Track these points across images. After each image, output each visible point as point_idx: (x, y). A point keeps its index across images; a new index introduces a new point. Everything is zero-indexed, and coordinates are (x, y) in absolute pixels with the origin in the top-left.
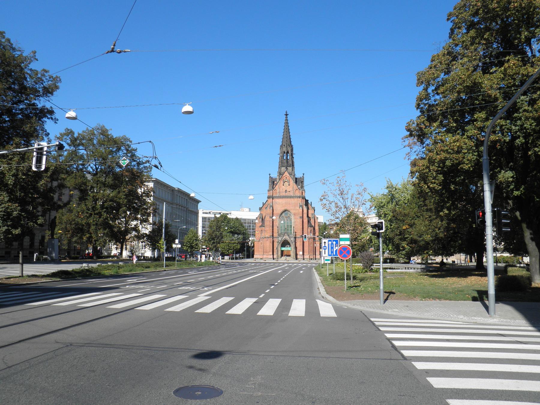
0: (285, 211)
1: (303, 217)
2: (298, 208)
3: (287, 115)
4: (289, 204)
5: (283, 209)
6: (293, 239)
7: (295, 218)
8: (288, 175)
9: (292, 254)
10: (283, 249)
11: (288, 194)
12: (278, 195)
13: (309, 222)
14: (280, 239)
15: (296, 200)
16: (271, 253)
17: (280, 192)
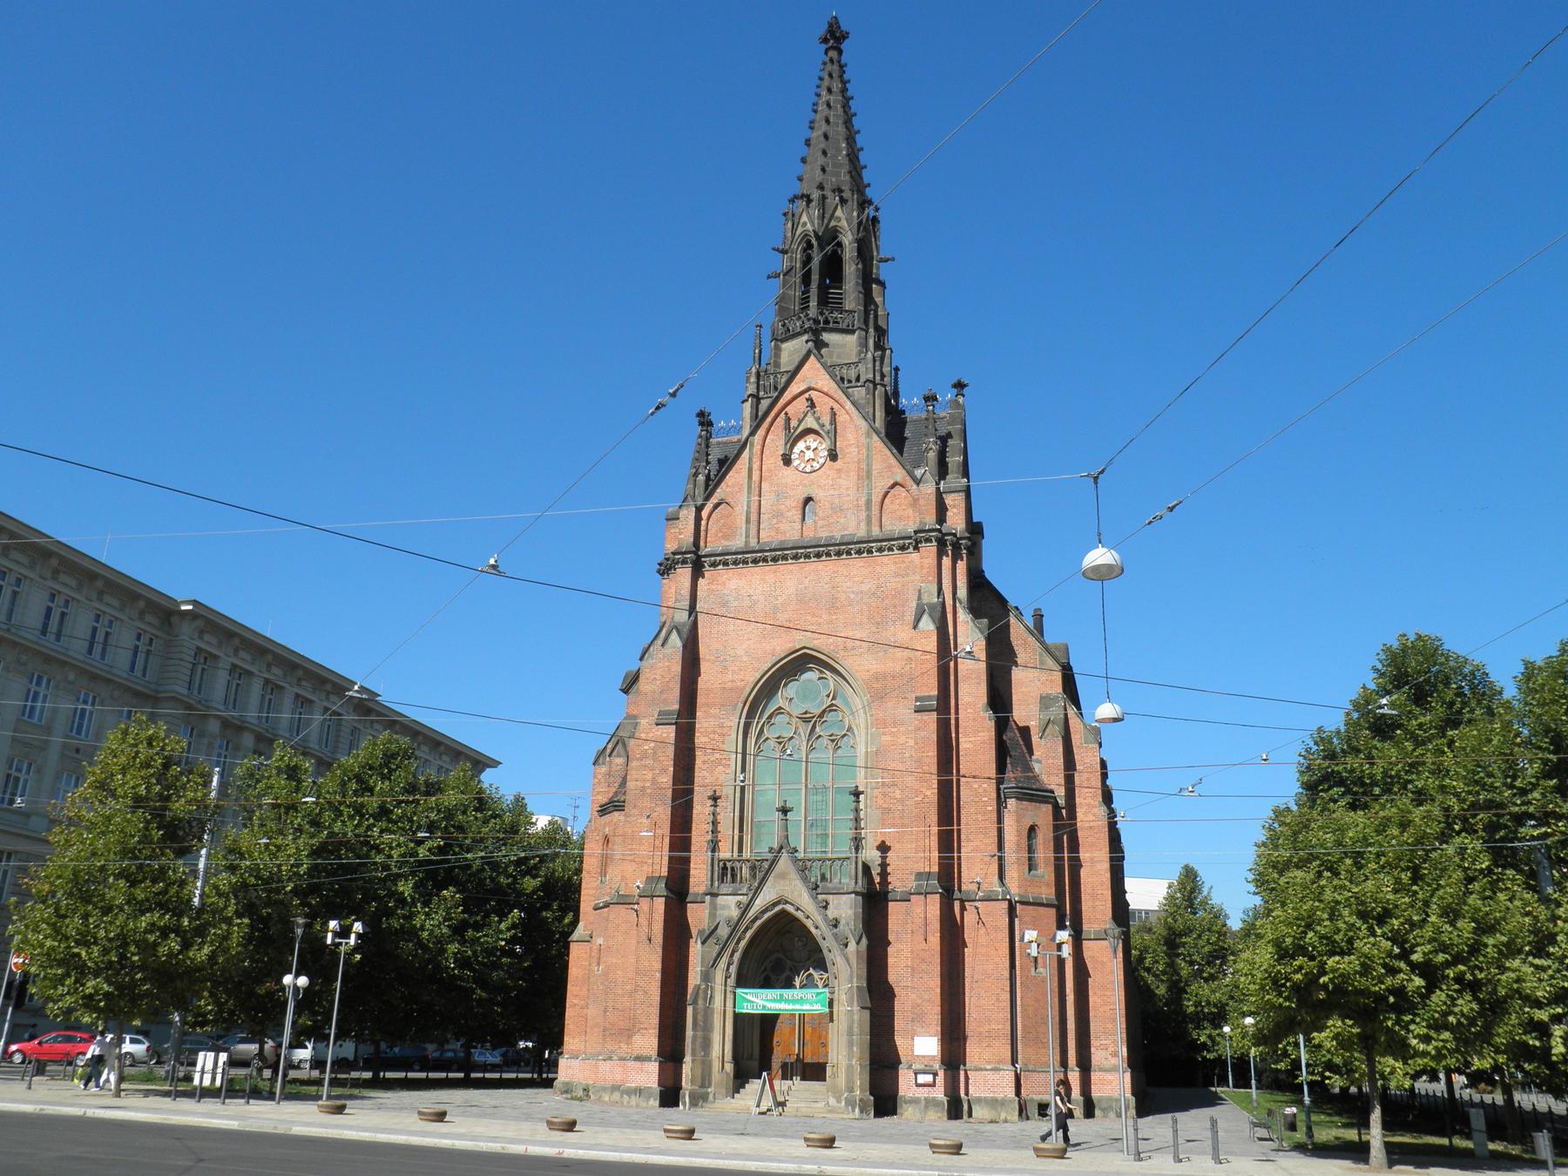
0: (798, 664)
1: (944, 703)
2: (903, 634)
3: (835, 37)
4: (834, 605)
5: (781, 646)
6: (846, 908)
7: (881, 723)
8: (825, 382)
9: (845, 1055)
10: (758, 1001)
11: (819, 528)
12: (738, 543)
13: (1010, 746)
14: (729, 905)
15: (887, 565)
16: (648, 1042)
17: (755, 517)
